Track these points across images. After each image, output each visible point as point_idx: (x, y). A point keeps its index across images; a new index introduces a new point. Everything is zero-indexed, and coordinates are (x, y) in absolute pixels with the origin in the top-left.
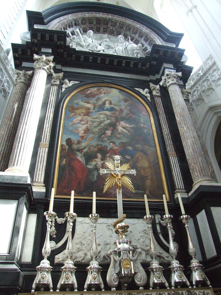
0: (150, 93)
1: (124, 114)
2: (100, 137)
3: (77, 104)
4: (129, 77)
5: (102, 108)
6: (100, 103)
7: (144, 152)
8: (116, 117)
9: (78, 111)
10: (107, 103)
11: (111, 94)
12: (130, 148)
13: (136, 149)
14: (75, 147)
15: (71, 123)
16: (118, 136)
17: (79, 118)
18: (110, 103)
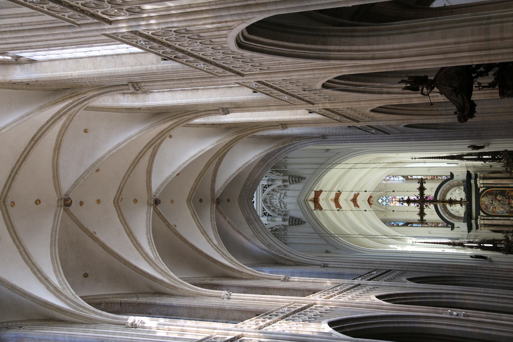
0: (482, 187)
1: (494, 197)
2: (504, 205)
3: (491, 211)
4: (474, 194)
5: (492, 204)
6: (490, 204)
7: (508, 193)
8: (495, 200)
9: (495, 210)
10: (489, 202)
11: (485, 200)
12: (507, 197)
13: (507, 195)
14: (508, 211)
15: (500, 212)
16: (503, 199)
17: (497, 210)
18: (489, 201)
